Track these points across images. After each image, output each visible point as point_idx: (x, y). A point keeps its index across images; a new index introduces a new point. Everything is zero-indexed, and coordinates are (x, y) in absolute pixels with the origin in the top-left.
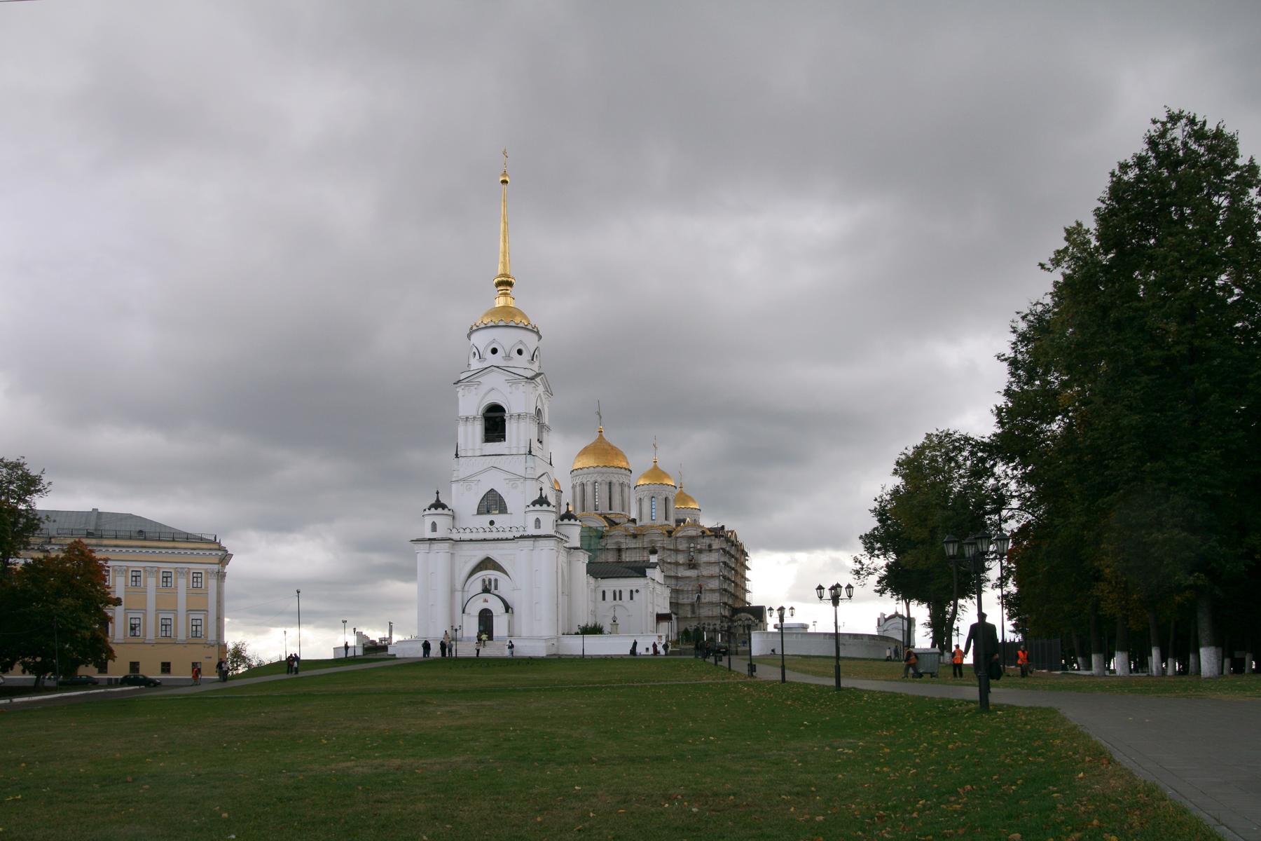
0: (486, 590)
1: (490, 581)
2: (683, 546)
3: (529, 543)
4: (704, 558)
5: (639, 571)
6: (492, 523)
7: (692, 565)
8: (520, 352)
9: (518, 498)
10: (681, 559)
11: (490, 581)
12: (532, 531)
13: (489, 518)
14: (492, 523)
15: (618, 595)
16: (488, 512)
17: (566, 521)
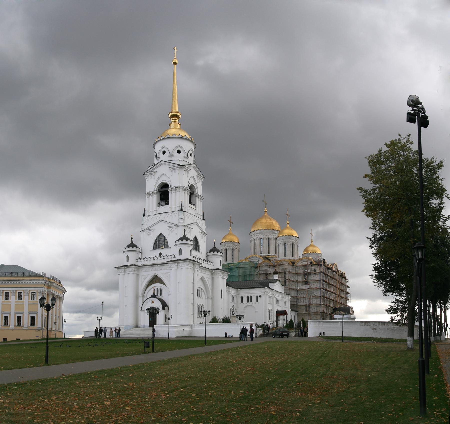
0: (154, 296)
1: (158, 289)
2: (301, 271)
3: (174, 265)
4: (313, 278)
5: (265, 285)
6: (160, 254)
7: (306, 283)
8: (179, 152)
9: (172, 238)
10: (300, 279)
11: (158, 289)
12: (178, 257)
13: (159, 251)
14: (160, 254)
15: (250, 299)
16: (159, 248)
17: (212, 253)
